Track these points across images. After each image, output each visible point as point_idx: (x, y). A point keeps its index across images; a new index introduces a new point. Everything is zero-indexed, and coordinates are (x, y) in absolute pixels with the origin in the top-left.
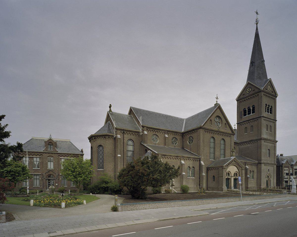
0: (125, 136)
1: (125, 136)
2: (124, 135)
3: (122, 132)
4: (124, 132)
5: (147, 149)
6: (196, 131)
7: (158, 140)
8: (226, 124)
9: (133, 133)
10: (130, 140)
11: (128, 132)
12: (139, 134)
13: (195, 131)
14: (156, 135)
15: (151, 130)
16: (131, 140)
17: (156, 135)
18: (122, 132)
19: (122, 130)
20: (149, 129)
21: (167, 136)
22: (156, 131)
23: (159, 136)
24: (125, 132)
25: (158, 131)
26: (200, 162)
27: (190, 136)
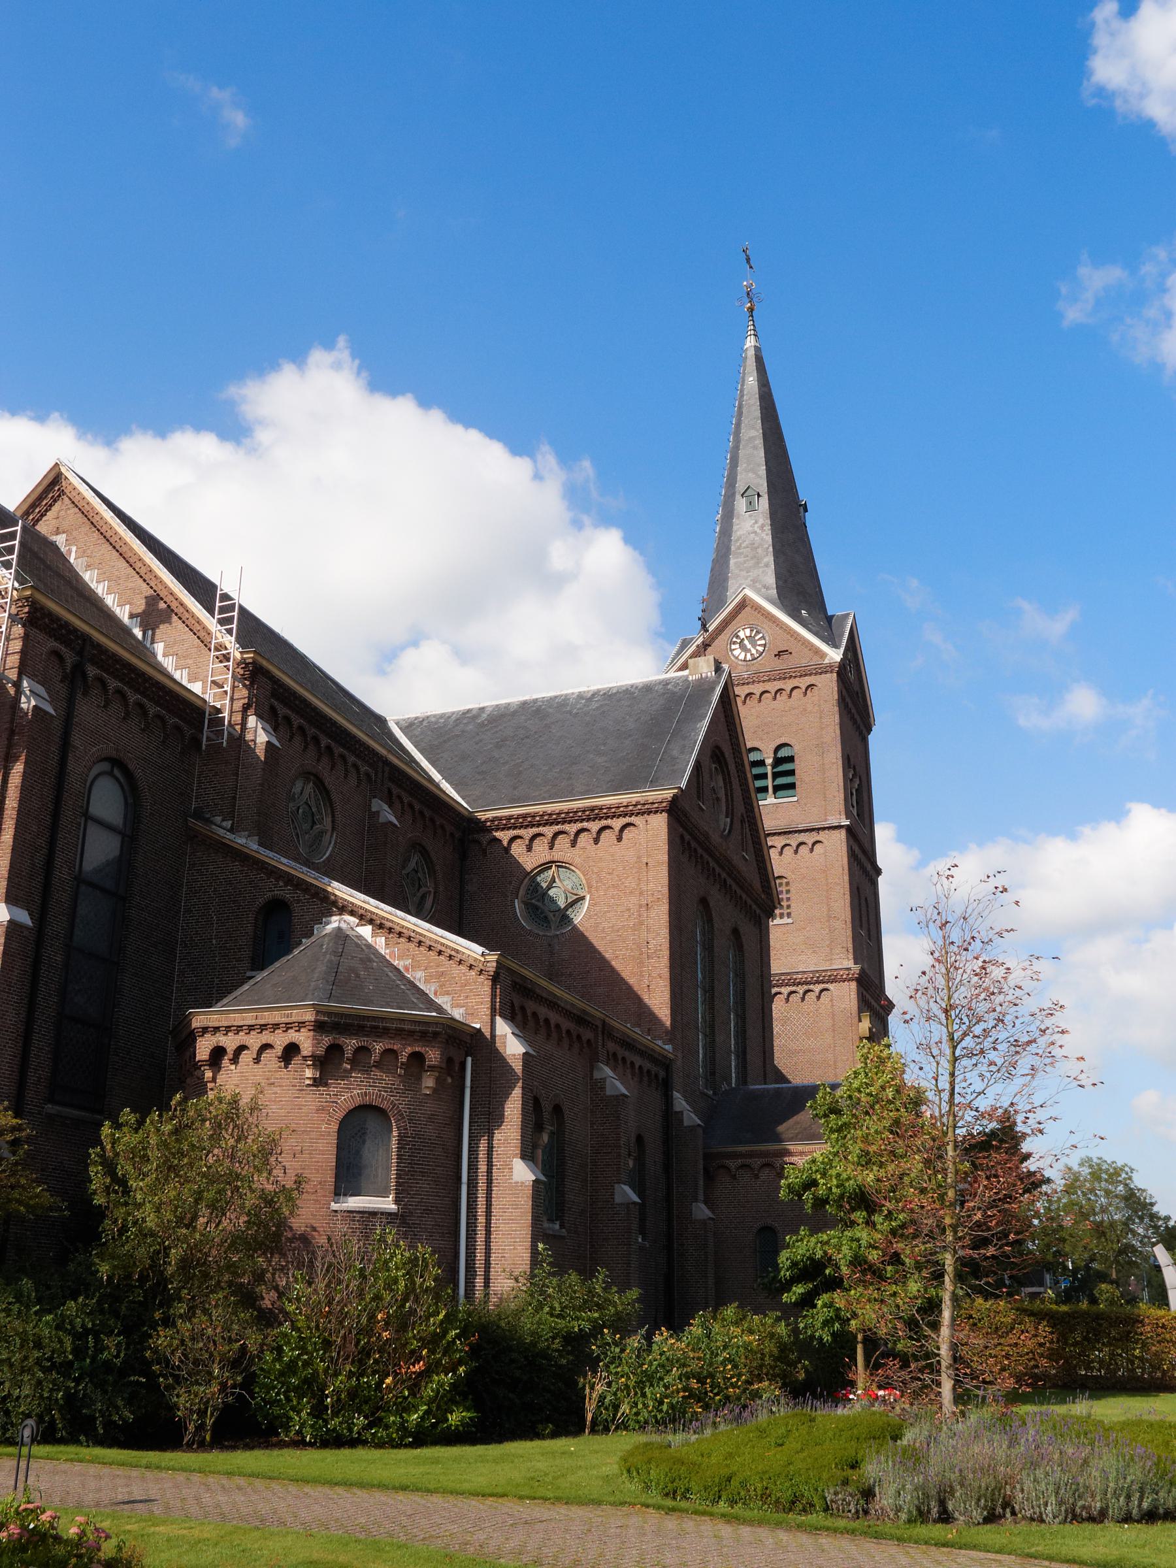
0: (87, 710)
1: (87, 710)
2: (79, 696)
3: (70, 658)
4: (79, 669)
5: (287, 893)
6: (617, 823)
7: (322, 833)
8: (742, 822)
9: (153, 709)
10: (111, 774)
11: (113, 684)
12: (188, 732)
13: (604, 823)
14: (320, 784)
15: (297, 721)
16: (116, 772)
17: (320, 784)
18: (70, 658)
19: (67, 643)
20: (282, 710)
21: (388, 815)
22: (325, 741)
23: (334, 796)
24: (92, 671)
25: (338, 750)
26: (668, 1100)
27: (541, 853)
